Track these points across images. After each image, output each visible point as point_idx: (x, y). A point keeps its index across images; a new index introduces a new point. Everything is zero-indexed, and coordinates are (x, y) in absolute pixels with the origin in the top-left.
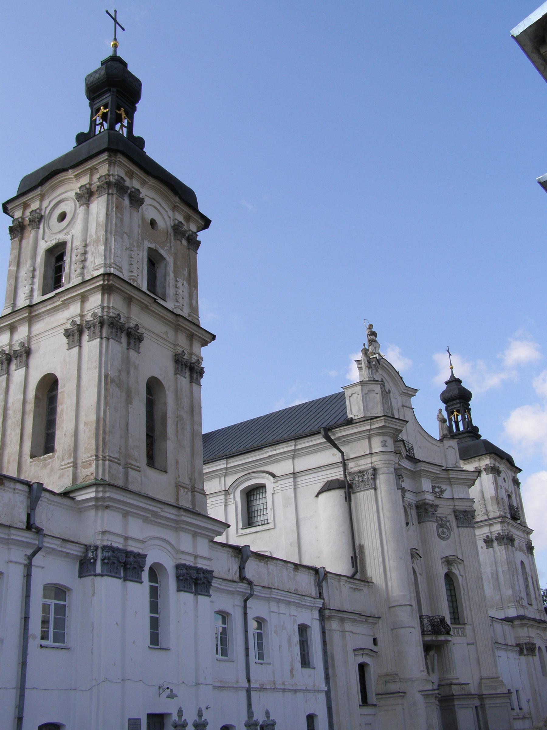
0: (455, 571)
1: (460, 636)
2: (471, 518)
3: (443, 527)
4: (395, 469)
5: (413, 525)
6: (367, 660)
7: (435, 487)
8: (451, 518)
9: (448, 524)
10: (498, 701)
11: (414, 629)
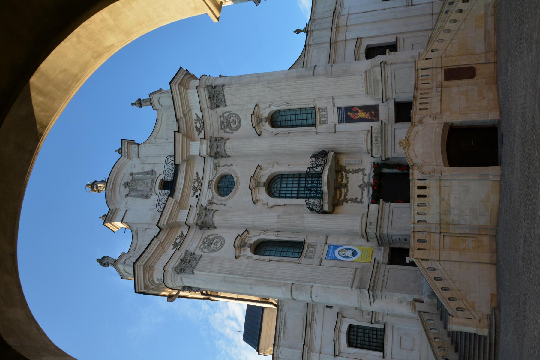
0: (266, 113)
1: (327, 114)
2: (214, 90)
3: (229, 122)
4: (178, 273)
5: (231, 165)
6: (345, 329)
7: (196, 127)
8: (220, 110)
9: (226, 115)
10: (389, 80)
11: (314, 288)
